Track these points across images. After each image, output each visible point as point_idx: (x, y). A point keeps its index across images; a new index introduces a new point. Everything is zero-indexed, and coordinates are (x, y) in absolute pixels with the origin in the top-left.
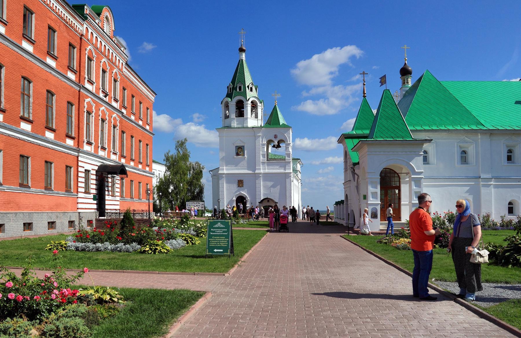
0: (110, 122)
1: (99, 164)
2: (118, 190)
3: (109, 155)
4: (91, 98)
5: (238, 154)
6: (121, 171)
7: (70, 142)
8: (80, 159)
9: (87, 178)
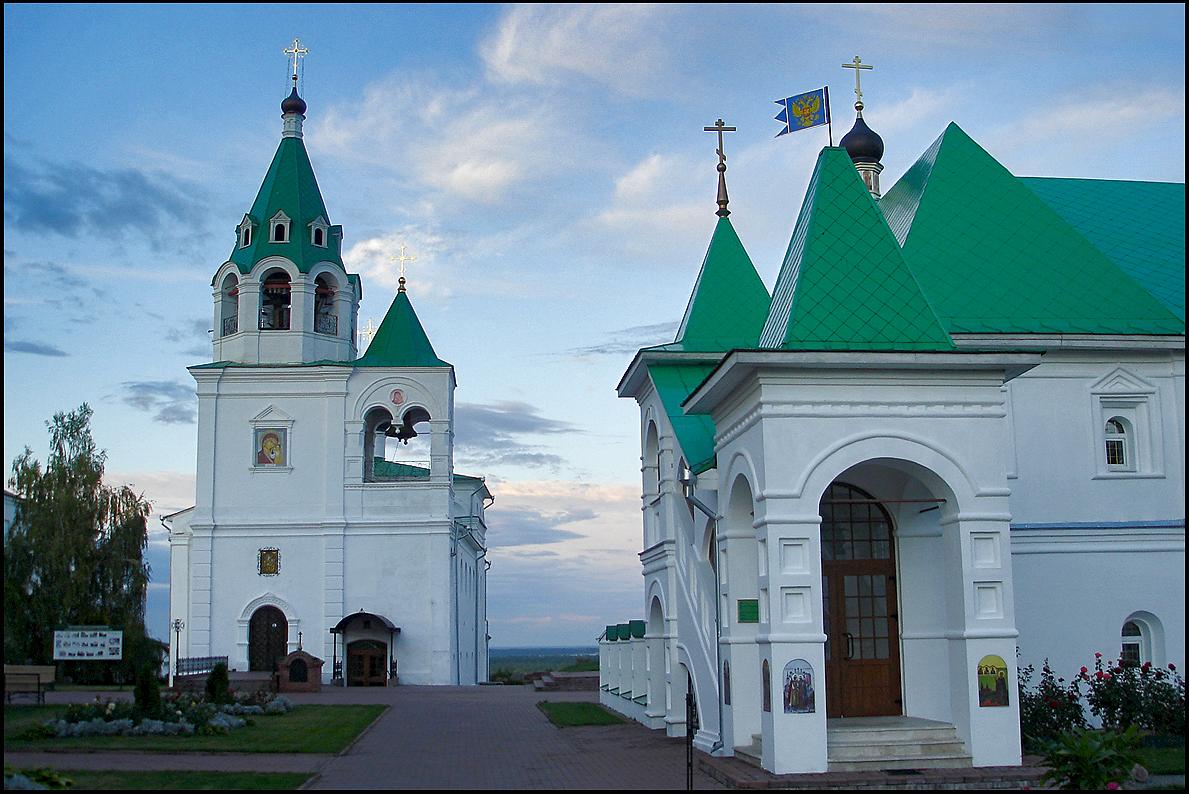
5: (262, 459)
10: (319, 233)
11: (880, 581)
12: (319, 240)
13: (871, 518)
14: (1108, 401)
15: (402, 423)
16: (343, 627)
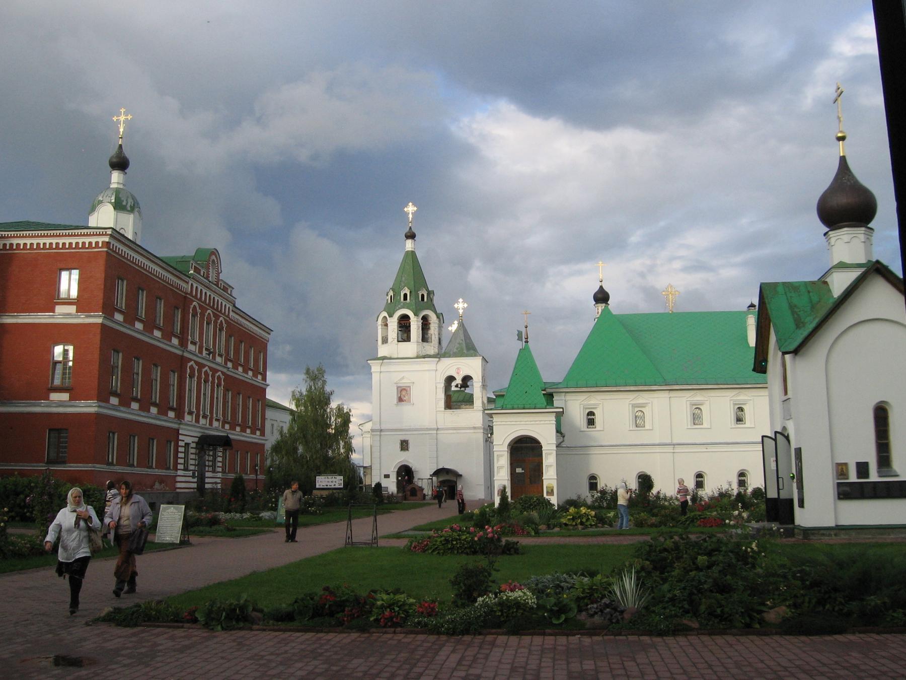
0: (213, 383)
1: (199, 435)
2: (220, 464)
3: (211, 424)
4: (195, 362)
6: (226, 442)
7: (171, 414)
8: (180, 432)
9: (186, 453)
16: (438, 473)
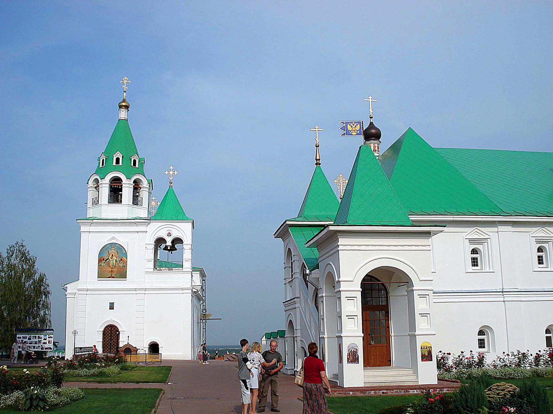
10: (135, 161)
11: (381, 314)
12: (135, 164)
13: (380, 290)
14: (472, 241)
15: (171, 244)
